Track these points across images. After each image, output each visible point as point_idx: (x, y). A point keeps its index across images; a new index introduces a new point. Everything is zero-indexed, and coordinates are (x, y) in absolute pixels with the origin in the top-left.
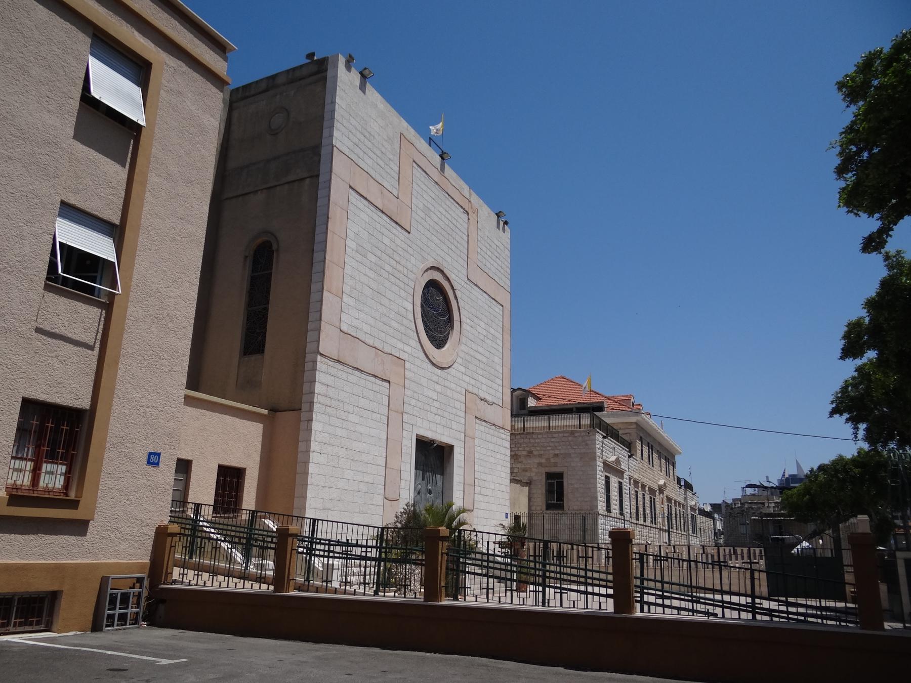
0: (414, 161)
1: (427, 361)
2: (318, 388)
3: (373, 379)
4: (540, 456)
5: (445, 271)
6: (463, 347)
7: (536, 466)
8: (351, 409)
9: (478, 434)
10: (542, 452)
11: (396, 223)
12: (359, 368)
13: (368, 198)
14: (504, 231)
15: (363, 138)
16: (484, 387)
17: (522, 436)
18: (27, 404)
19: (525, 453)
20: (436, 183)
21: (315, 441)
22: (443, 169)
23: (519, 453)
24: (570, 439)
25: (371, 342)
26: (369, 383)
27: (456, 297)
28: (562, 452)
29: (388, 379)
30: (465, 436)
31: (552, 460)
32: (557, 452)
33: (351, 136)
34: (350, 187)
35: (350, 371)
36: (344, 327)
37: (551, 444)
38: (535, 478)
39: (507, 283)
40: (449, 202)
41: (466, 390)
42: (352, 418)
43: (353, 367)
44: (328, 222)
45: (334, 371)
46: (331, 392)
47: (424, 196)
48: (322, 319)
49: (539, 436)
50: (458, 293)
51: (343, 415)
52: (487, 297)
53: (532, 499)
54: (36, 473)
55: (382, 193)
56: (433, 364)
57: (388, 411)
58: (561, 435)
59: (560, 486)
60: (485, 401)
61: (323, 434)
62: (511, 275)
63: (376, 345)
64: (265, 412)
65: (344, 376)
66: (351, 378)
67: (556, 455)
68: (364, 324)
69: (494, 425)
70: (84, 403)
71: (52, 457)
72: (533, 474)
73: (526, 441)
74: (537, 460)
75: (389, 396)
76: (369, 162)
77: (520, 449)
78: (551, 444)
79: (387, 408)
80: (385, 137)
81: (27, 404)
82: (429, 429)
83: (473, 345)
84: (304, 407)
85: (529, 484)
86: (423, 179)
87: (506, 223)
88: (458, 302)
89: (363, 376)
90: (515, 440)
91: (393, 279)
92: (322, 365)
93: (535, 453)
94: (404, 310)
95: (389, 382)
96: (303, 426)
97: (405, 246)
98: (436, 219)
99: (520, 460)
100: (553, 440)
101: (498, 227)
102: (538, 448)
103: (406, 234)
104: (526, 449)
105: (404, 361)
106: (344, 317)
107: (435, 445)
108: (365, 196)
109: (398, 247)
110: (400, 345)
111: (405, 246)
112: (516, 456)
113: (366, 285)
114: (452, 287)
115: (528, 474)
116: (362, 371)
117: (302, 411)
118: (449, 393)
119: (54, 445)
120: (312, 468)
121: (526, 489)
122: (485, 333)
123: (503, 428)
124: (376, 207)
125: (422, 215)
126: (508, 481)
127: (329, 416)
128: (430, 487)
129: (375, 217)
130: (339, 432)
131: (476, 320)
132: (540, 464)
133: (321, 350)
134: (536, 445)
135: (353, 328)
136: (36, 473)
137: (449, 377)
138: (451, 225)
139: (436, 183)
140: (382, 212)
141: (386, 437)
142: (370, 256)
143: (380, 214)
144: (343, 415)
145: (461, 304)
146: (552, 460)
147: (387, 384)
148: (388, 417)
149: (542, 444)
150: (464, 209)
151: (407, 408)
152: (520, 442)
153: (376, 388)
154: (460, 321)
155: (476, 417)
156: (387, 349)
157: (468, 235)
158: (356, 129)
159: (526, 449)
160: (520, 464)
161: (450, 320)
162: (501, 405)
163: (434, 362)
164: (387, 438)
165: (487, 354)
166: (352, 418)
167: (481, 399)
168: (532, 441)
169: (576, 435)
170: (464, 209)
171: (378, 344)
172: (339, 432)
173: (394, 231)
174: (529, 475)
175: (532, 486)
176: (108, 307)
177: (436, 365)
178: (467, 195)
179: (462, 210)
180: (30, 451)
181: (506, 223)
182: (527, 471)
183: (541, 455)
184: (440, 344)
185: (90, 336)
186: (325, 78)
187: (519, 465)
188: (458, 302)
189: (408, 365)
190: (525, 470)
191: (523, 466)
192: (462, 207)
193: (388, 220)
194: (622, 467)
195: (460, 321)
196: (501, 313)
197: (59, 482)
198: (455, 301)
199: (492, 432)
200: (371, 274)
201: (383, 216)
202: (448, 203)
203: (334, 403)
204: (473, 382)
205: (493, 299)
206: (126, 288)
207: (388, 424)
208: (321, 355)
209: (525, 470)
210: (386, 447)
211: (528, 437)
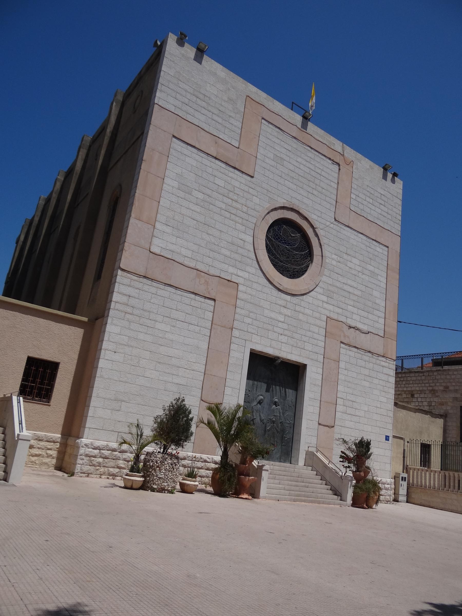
0: (263, 118)
1: (270, 286)
3: (193, 296)
4: (456, 391)
5: (300, 211)
6: (324, 279)
7: (451, 400)
8: (159, 318)
9: (342, 357)
10: (457, 388)
11: (235, 168)
12: (172, 284)
13: (197, 146)
14: (393, 181)
15: (195, 98)
16: (355, 317)
17: (439, 372)
19: (442, 388)
20: (295, 138)
21: (109, 340)
22: (304, 126)
23: (436, 388)
25: (192, 265)
26: (186, 298)
27: (317, 235)
29: (213, 298)
30: (324, 357)
33: (178, 96)
34: (174, 136)
35: (162, 286)
36: (154, 249)
38: (450, 412)
39: (397, 229)
40: (312, 154)
41: (327, 317)
42: (158, 326)
43: (165, 284)
44: (142, 163)
45: (140, 285)
46: (132, 302)
47: (276, 148)
48: (126, 240)
49: (455, 373)
50: (320, 232)
52: (364, 238)
53: (448, 431)
55: (216, 143)
56: (279, 290)
57: (212, 325)
60: (356, 329)
61: (121, 336)
62: (402, 221)
63: (198, 267)
65: (153, 290)
66: (160, 292)
68: (182, 249)
69: (370, 352)
72: (449, 408)
73: (442, 377)
74: (452, 395)
75: (214, 313)
76: (203, 118)
77: (437, 384)
79: (211, 322)
80: (226, 99)
82: (270, 347)
83: (340, 278)
85: (444, 416)
86: (275, 134)
87: (395, 175)
88: (319, 240)
89: (179, 292)
90: (433, 376)
91: (228, 215)
93: (451, 388)
94: (241, 241)
95: (214, 300)
97: (246, 188)
98: (292, 167)
99: (437, 394)
102: (454, 384)
103: (249, 178)
104: (443, 384)
105: (237, 284)
107: (280, 361)
108: (194, 145)
109: (235, 188)
110: (231, 270)
111: (246, 188)
112: (433, 390)
113: (189, 217)
114: (312, 226)
115: (444, 408)
116: (177, 288)
117: (105, 316)
118: (301, 316)
120: (102, 363)
121: (440, 422)
122: (359, 269)
123: (383, 356)
124: (208, 154)
125: (273, 163)
126: (391, 405)
127: (130, 322)
128: (276, 400)
129: (208, 163)
131: (345, 256)
132: (455, 399)
134: (451, 381)
135: (167, 250)
137: (303, 304)
138: (313, 173)
139: (295, 138)
140: (216, 158)
141: (207, 347)
142: (195, 193)
143: (214, 160)
145: (323, 240)
147: (212, 303)
148: (211, 330)
149: (457, 380)
150: (333, 160)
151: (236, 324)
152: (437, 378)
153: (193, 303)
154: (322, 256)
155: (341, 342)
156: (212, 272)
157: (338, 183)
158: (186, 91)
159: (443, 384)
160: (437, 398)
161: (310, 255)
162: (382, 335)
163: (281, 288)
164: (208, 348)
165: (363, 288)
166: (158, 326)
167: (350, 327)
168: (448, 377)
170: (333, 160)
171: (200, 267)
172: (141, 336)
173: (231, 174)
174: (445, 409)
175: (448, 419)
177: (284, 291)
178: (340, 150)
179: (330, 161)
181: (395, 175)
182: (443, 405)
183: (457, 390)
184: (293, 275)
187: (436, 399)
188: (319, 240)
189: (241, 288)
190: (442, 404)
191: (440, 400)
192: (330, 159)
193: (223, 165)
195: (322, 256)
196: (386, 253)
198: (316, 239)
199: (374, 360)
200: (198, 209)
201: (217, 162)
202: (310, 154)
203: (136, 312)
204: (340, 311)
205: (373, 240)
207: (210, 336)
208: (123, 270)
209: (442, 404)
210: (206, 356)
211: (445, 373)
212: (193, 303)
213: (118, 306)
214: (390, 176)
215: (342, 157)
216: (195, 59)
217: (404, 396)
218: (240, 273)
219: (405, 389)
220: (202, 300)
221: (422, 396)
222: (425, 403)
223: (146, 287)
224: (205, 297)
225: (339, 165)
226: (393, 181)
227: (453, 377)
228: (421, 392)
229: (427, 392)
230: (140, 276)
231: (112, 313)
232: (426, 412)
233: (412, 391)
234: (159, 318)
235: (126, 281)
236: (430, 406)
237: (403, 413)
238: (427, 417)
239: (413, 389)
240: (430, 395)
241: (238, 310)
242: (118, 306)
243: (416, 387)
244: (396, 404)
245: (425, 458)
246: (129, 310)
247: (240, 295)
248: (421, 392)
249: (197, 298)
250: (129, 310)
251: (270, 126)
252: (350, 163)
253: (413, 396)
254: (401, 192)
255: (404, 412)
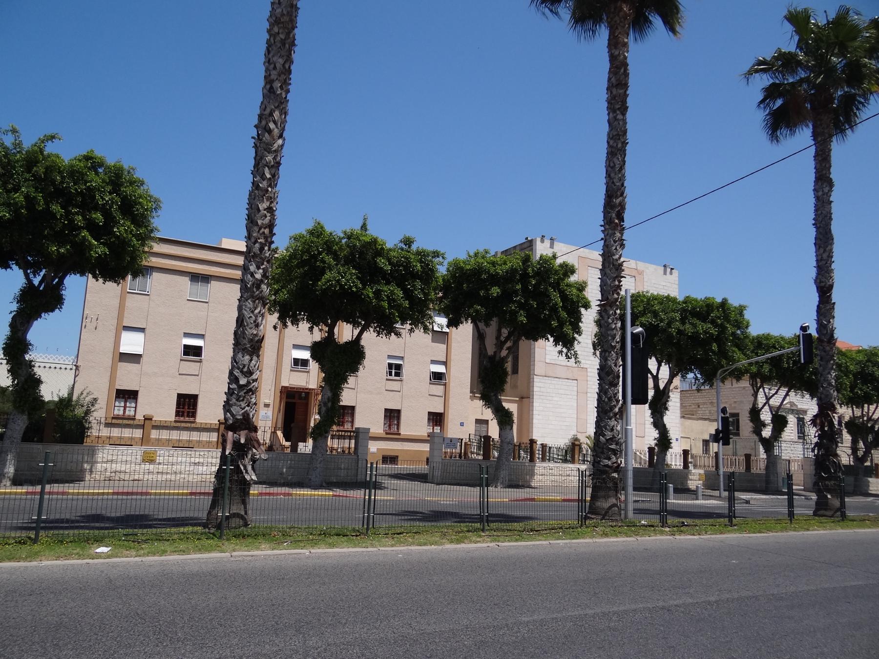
2: (535, 389)
8: (554, 395)
10: (726, 400)
18: (429, 413)
24: (743, 391)
28: (739, 400)
31: (733, 405)
32: (735, 400)
36: (548, 361)
37: (732, 395)
42: (555, 399)
45: (544, 381)
46: (542, 390)
51: (550, 398)
54: (433, 429)
58: (737, 389)
59: (738, 421)
64: (518, 399)
65: (549, 382)
66: (553, 382)
67: (735, 402)
70: (442, 411)
71: (436, 425)
78: (732, 395)
81: (429, 413)
84: (531, 397)
92: (536, 379)
96: (531, 404)
100: (733, 392)
101: (665, 273)
106: (547, 357)
112: (712, 402)
119: (436, 422)
120: (535, 421)
130: (548, 405)
133: (535, 373)
136: (433, 429)
144: (550, 398)
146: (733, 405)
153: (568, 384)
166: (555, 399)
169: (747, 389)
172: (548, 405)
176: (445, 385)
180: (431, 424)
185: (441, 393)
186: (532, 249)
194: (799, 407)
197: (439, 431)
203: (544, 394)
206: (449, 381)
212: (568, 384)
213: (537, 393)
214: (668, 270)
215: (636, 271)
216: (550, 248)
217: (693, 407)
218: (587, 362)
219: (694, 402)
220: (571, 381)
221: (705, 406)
222: (707, 412)
223: (547, 381)
224: (573, 380)
225: (635, 277)
226: (671, 273)
227: (724, 393)
228: (704, 403)
229: (708, 403)
230: (543, 376)
231: (535, 397)
232: (705, 419)
233: (698, 403)
234: (554, 395)
235: (538, 380)
236: (710, 413)
237: (688, 422)
238: (707, 422)
239: (699, 402)
240: (710, 406)
241: (588, 382)
242: (537, 393)
243: (700, 401)
244: (682, 417)
245: (706, 449)
246: (541, 394)
247: (589, 374)
248: (704, 403)
249: (569, 381)
250: (541, 394)
251: (593, 269)
252: (641, 273)
253: (699, 406)
254: (677, 279)
255: (690, 421)
